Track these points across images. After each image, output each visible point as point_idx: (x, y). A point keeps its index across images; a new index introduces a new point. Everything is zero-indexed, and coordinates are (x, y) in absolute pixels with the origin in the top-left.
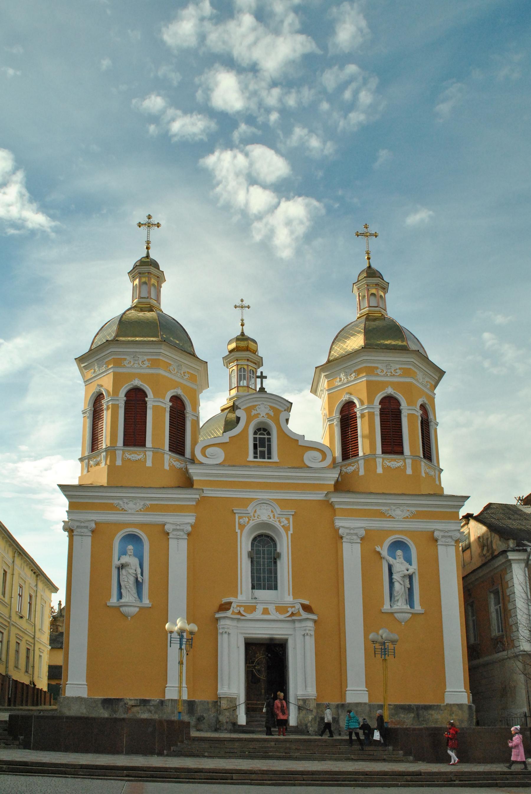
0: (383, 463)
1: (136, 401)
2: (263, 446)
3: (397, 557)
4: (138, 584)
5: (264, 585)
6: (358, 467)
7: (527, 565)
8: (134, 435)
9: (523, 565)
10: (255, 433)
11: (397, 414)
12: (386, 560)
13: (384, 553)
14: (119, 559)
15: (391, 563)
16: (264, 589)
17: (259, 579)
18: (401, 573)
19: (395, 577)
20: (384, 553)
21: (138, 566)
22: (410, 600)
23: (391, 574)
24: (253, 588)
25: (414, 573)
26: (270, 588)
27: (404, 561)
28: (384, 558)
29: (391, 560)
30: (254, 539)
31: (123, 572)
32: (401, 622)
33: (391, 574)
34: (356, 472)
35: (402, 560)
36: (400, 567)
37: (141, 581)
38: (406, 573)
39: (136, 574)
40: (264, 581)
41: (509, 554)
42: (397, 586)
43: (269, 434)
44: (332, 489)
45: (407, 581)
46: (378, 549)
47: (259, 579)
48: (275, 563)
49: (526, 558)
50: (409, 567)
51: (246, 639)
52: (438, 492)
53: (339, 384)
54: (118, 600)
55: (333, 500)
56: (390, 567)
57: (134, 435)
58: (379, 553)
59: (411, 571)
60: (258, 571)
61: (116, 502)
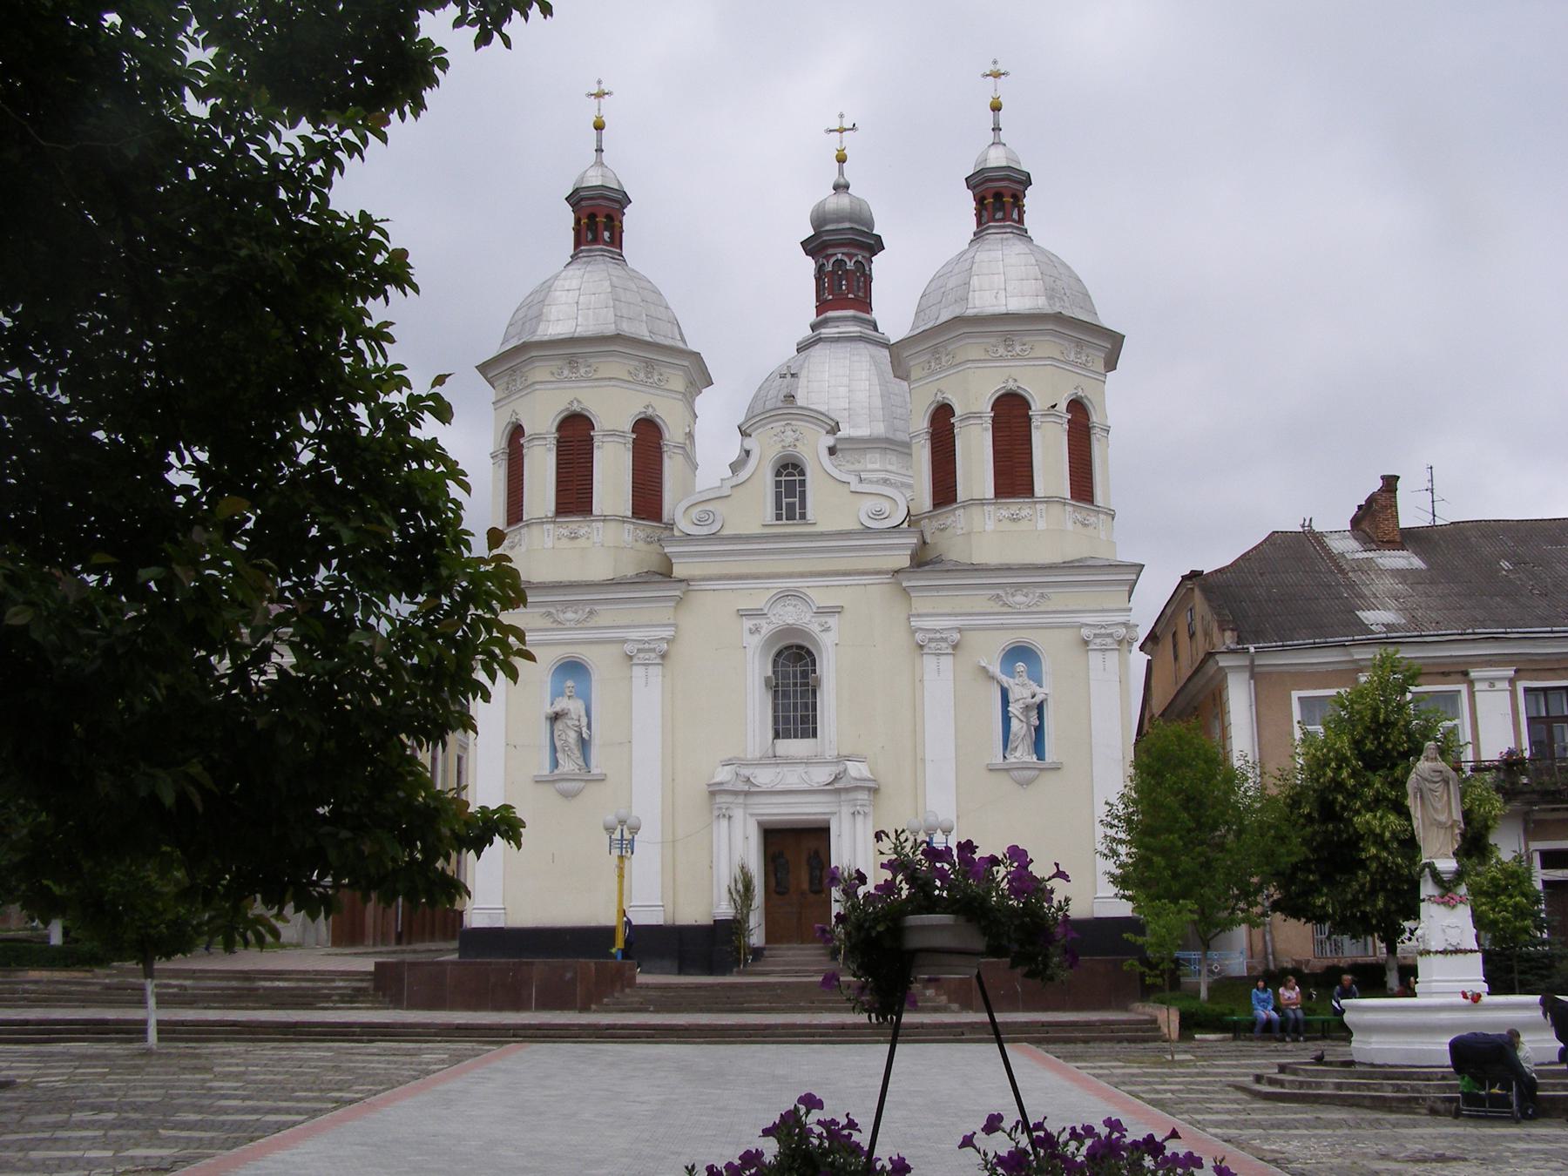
1: (575, 436)
2: (790, 494)
5: (796, 730)
6: (957, 519)
7: (1253, 676)
9: (1247, 675)
10: (778, 474)
13: (995, 669)
16: (796, 737)
17: (786, 720)
19: (1014, 709)
20: (995, 669)
21: (583, 713)
24: (777, 735)
26: (805, 735)
27: (1027, 681)
28: (993, 678)
29: (1006, 681)
30: (779, 654)
31: (559, 725)
35: (1025, 679)
36: (1021, 691)
40: (795, 723)
41: (1218, 657)
42: (1015, 724)
43: (802, 473)
44: (906, 562)
45: (1034, 714)
47: (786, 720)
48: (814, 693)
49: (1247, 663)
50: (1038, 690)
51: (760, 824)
52: (1104, 554)
55: (905, 584)
56: (1005, 693)
59: (1037, 700)
60: (786, 708)
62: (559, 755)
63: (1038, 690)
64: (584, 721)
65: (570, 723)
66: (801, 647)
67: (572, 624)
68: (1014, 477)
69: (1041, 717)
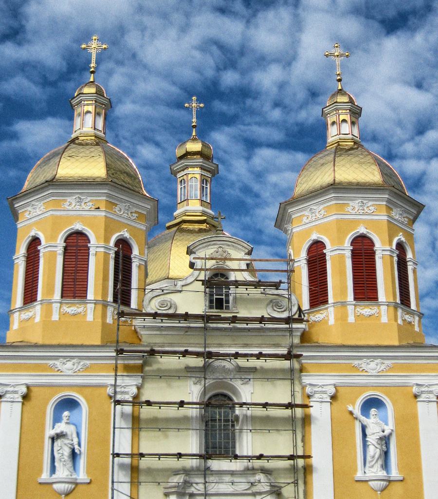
0: (355, 311)
3: (371, 416)
4: (74, 455)
6: (328, 315)
8: (74, 286)
11: (372, 254)
12: (360, 421)
13: (357, 412)
14: (53, 428)
15: (365, 423)
18: (376, 434)
19: (372, 439)
22: (386, 466)
23: (364, 435)
25: (390, 434)
28: (356, 418)
31: (58, 443)
32: (376, 491)
33: (364, 435)
34: (325, 321)
37: (78, 453)
38: (382, 434)
39: (72, 444)
46: (350, 408)
53: (307, 221)
54: (51, 475)
56: (364, 428)
57: (74, 286)
58: (351, 413)
59: (387, 433)
61: (51, 362)
62: (56, 464)
63: (386, 427)
64: (76, 440)
65: (67, 441)
66: (225, 396)
67: (70, 373)
68: (365, 289)
69: (387, 444)
